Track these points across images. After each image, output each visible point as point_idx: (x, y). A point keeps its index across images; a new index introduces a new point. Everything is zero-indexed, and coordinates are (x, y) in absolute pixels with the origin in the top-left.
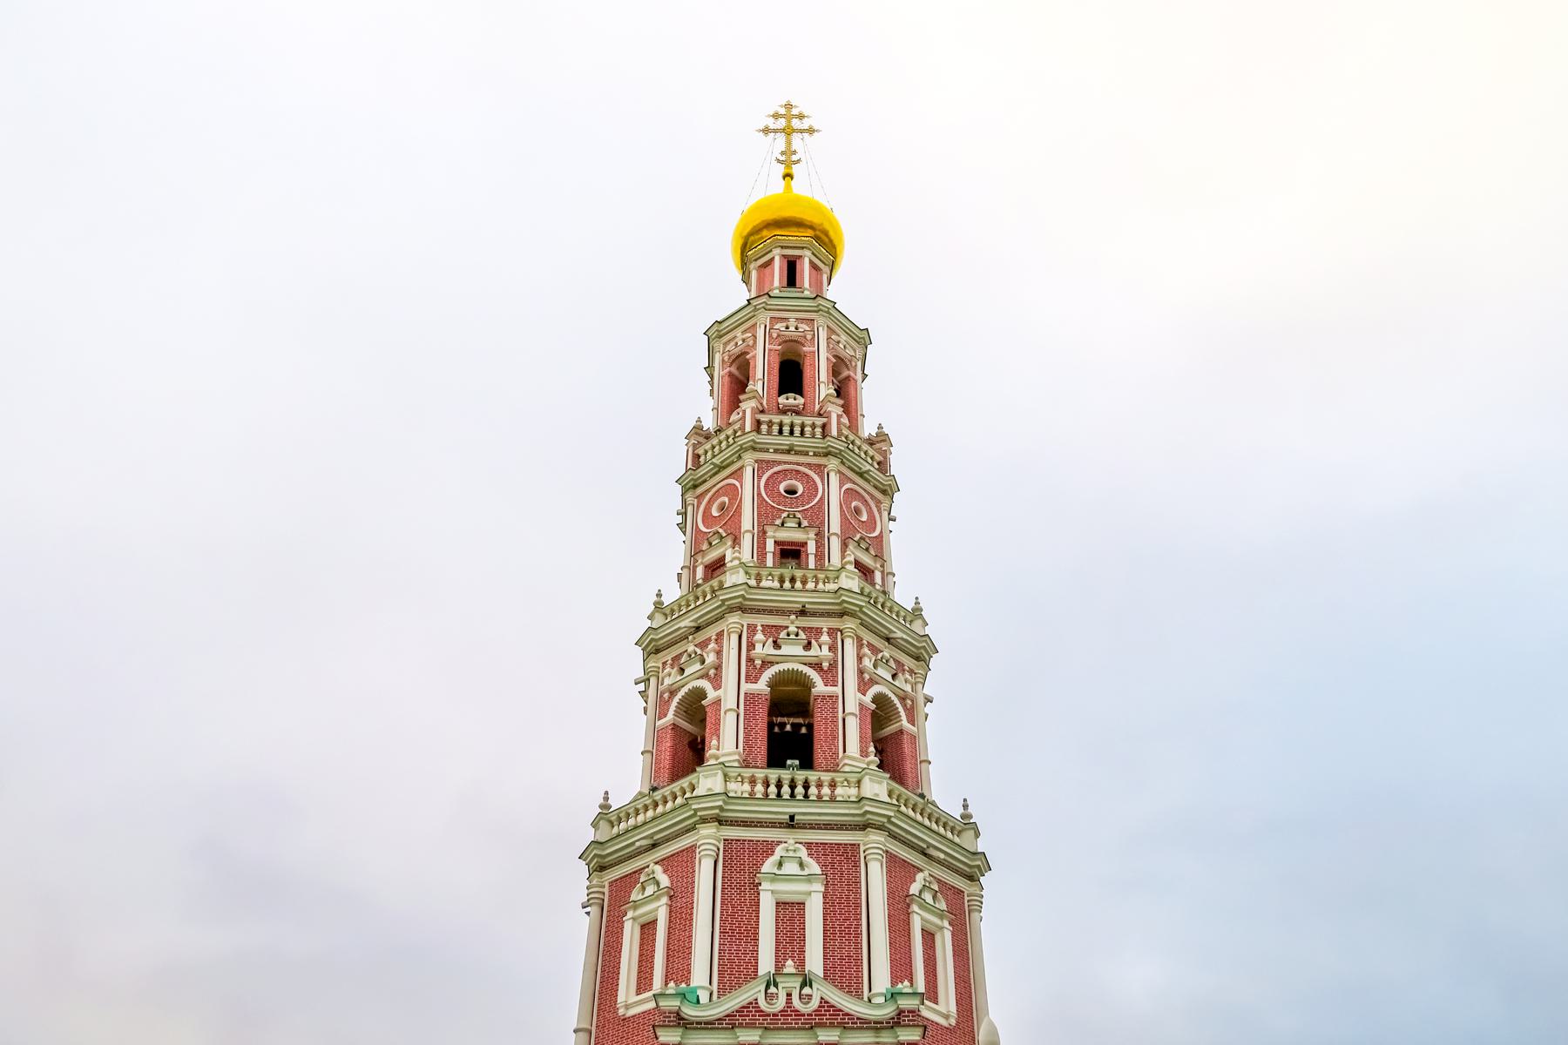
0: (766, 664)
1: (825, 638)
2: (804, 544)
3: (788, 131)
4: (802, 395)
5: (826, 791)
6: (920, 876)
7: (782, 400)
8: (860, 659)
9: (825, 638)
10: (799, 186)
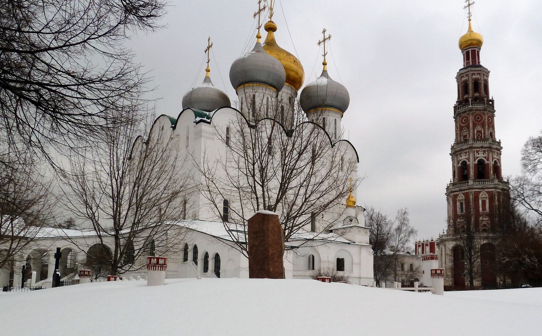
0: (460, 160)
6: (482, 192)
7: (465, 97)
8: (474, 155)
9: (467, 154)
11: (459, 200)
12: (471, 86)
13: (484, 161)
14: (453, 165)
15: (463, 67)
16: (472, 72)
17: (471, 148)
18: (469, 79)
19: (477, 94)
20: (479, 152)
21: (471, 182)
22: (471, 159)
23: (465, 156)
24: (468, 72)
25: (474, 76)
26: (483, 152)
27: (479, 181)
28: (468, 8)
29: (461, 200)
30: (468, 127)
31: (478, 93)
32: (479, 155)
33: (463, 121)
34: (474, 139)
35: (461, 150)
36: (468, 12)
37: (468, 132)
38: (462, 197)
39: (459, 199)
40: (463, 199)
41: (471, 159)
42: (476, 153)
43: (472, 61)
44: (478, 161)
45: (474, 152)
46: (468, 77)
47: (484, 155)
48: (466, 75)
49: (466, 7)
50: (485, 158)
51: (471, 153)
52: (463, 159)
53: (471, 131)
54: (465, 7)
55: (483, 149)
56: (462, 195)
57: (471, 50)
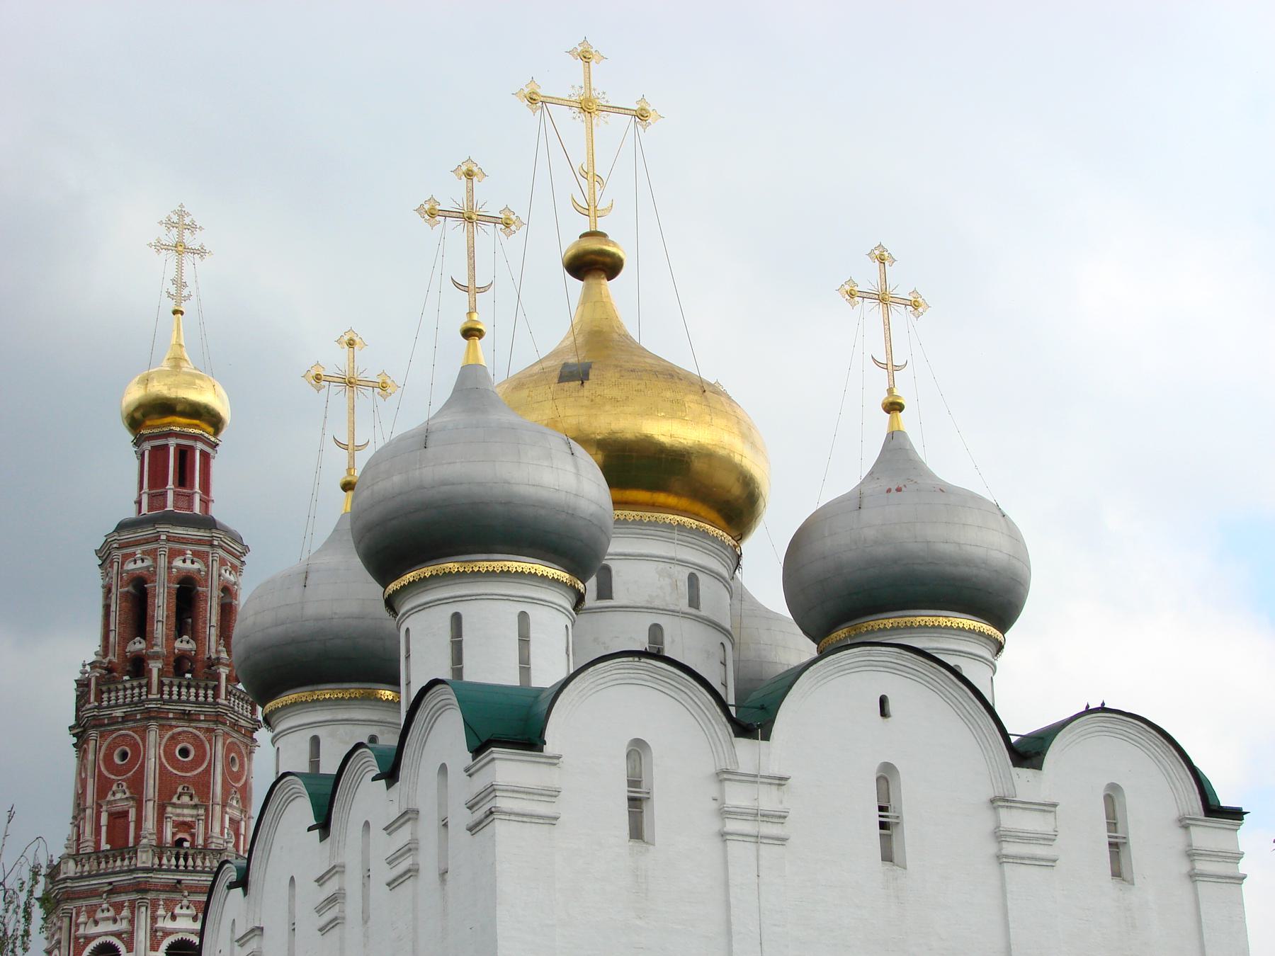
0: (89, 939)
2: (128, 812)
8: (154, 919)
9: (125, 913)
12: (162, 607)
15: (131, 513)
17: (141, 888)
19: (184, 645)
22: (142, 937)
24: (157, 539)
26: (192, 911)
31: (194, 637)
33: (117, 760)
34: (160, 849)
41: (142, 937)
42: (161, 912)
43: (176, 494)
46: (155, 560)
51: (143, 909)
52: (106, 934)
53: (150, 811)
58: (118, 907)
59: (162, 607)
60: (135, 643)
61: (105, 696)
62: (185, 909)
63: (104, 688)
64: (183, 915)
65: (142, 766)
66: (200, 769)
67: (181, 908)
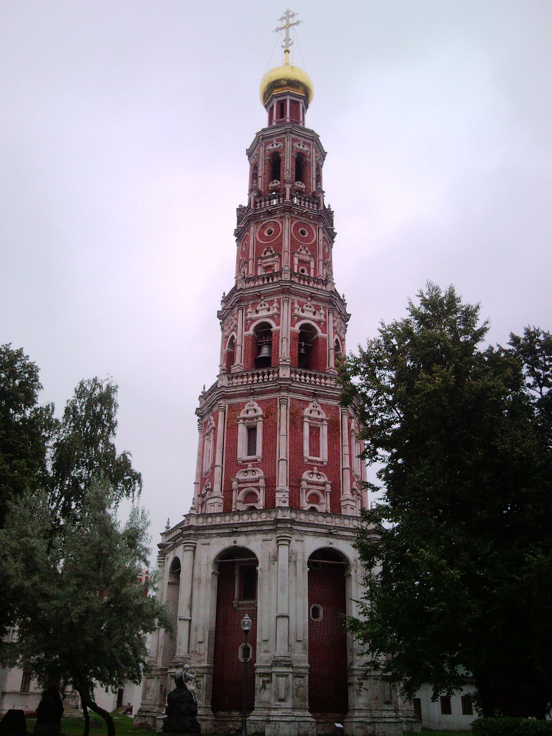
0: (253, 321)
1: (275, 305)
3: (288, 26)
4: (280, 181)
5: (266, 376)
6: (311, 405)
7: (271, 185)
8: (293, 310)
9: (275, 305)
10: (294, 58)
11: (244, 419)
12: (288, 164)
13: (315, 331)
14: (225, 338)
16: (293, 136)
17: (286, 291)
18: (284, 147)
19: (300, 185)
20: (305, 307)
21: (285, 373)
23: (269, 310)
25: (296, 145)
26: (313, 309)
27: (305, 375)
28: (284, 31)
29: (252, 419)
30: (278, 246)
32: (305, 315)
34: (293, 274)
35: (258, 296)
36: (284, 37)
37: (277, 257)
38: (255, 411)
39: (246, 416)
40: (257, 417)
42: (296, 306)
44: (302, 327)
45: (293, 304)
47: (317, 317)
48: (277, 140)
49: (281, 29)
50: (319, 322)
51: (286, 304)
53: (286, 257)
54: (278, 29)
55: (314, 302)
56: (256, 404)
57: (291, 101)
58: (271, 303)
59: (288, 164)
60: (273, 183)
61: (258, 205)
62: (308, 308)
63: (258, 200)
64: (307, 310)
65: (282, 234)
66: (311, 243)
67: (307, 306)
